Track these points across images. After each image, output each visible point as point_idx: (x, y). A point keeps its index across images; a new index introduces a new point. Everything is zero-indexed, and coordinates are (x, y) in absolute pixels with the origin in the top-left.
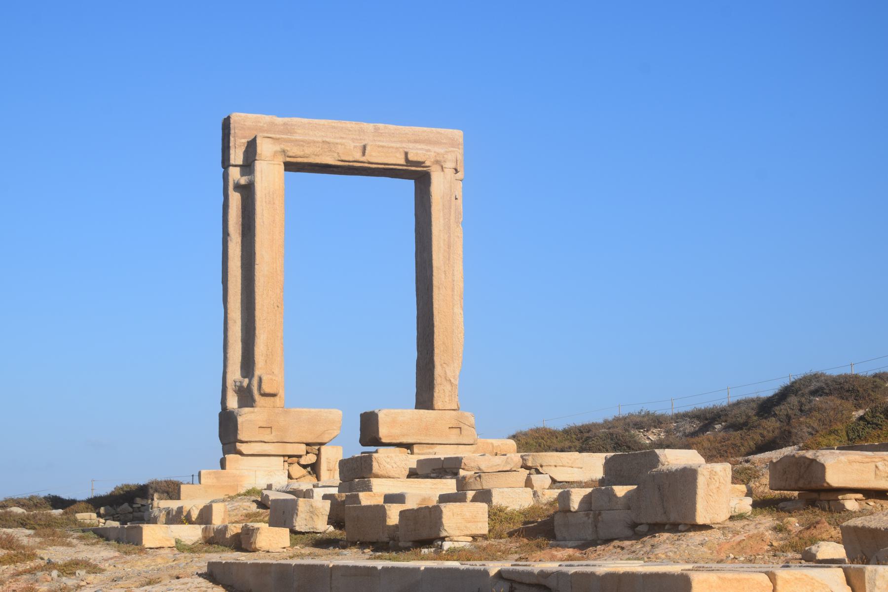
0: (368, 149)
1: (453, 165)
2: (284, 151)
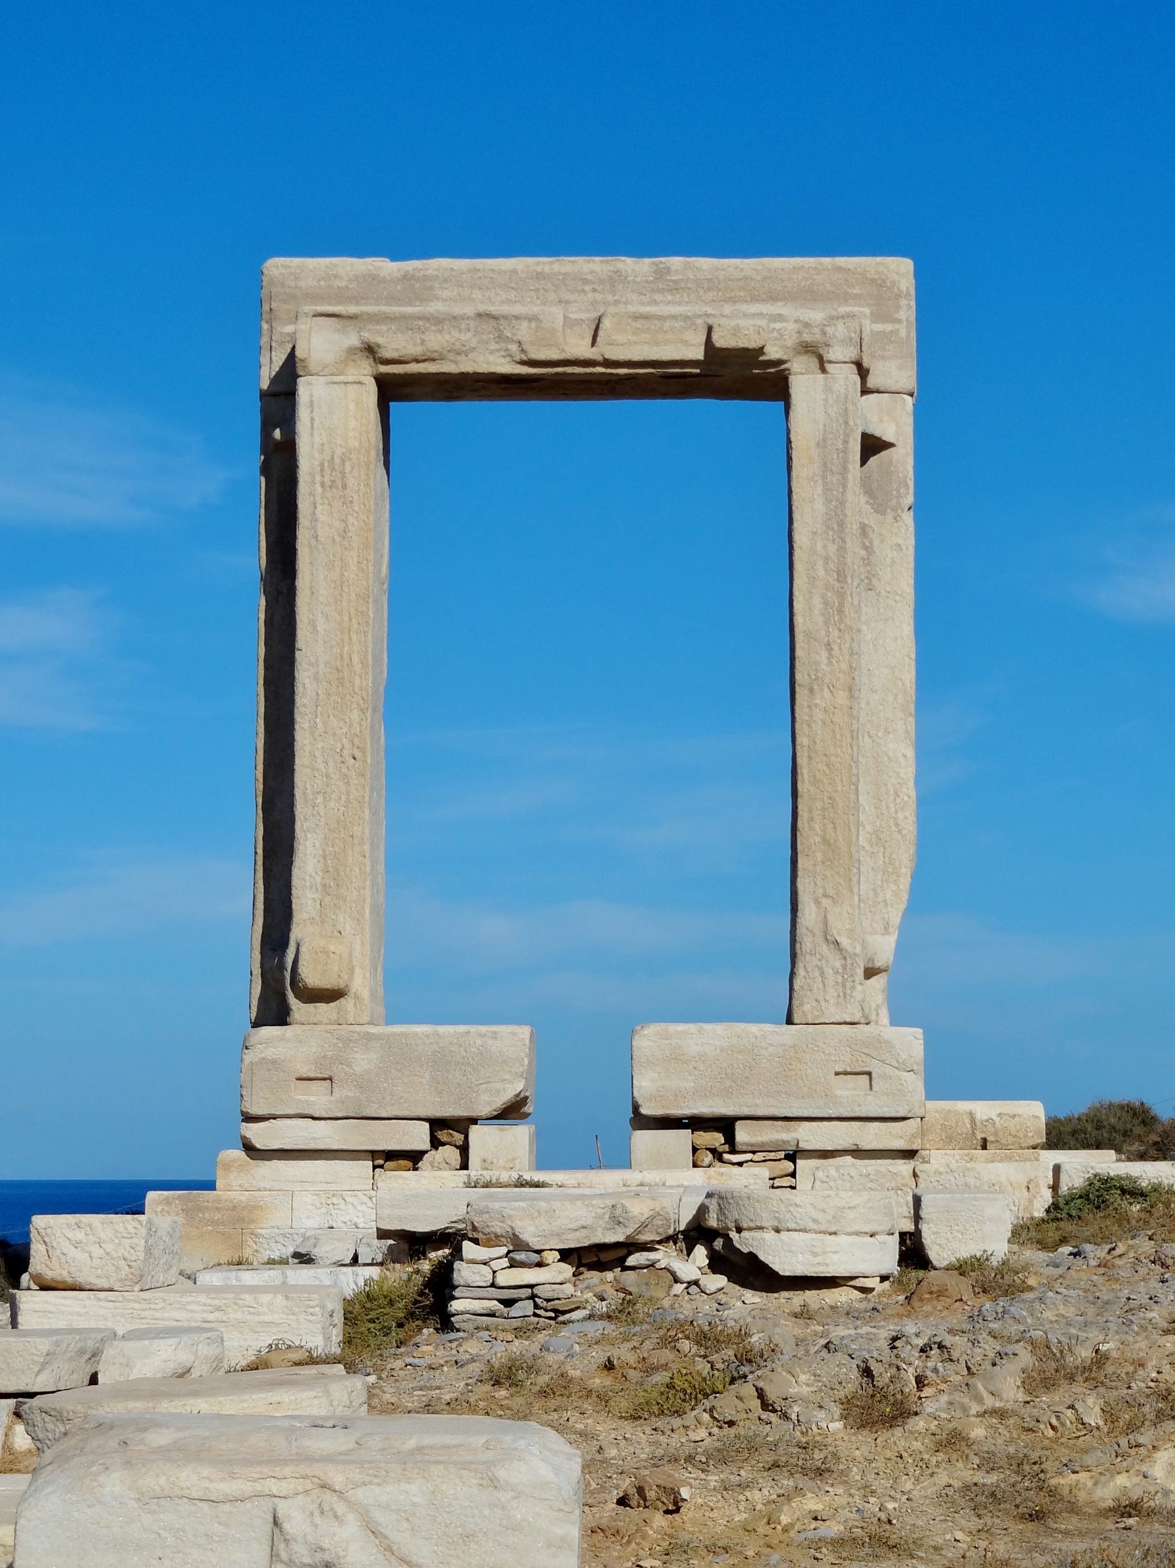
1: (851, 353)
2: (370, 350)
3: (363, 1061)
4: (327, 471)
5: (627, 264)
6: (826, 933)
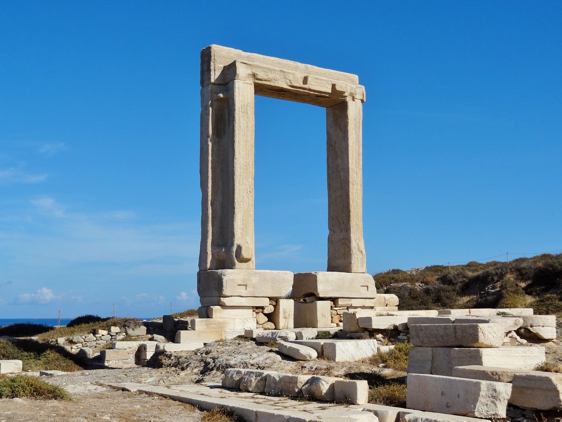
0: (309, 79)
1: (361, 97)
2: (254, 75)
3: (255, 280)
5: (299, 64)
6: (359, 249)
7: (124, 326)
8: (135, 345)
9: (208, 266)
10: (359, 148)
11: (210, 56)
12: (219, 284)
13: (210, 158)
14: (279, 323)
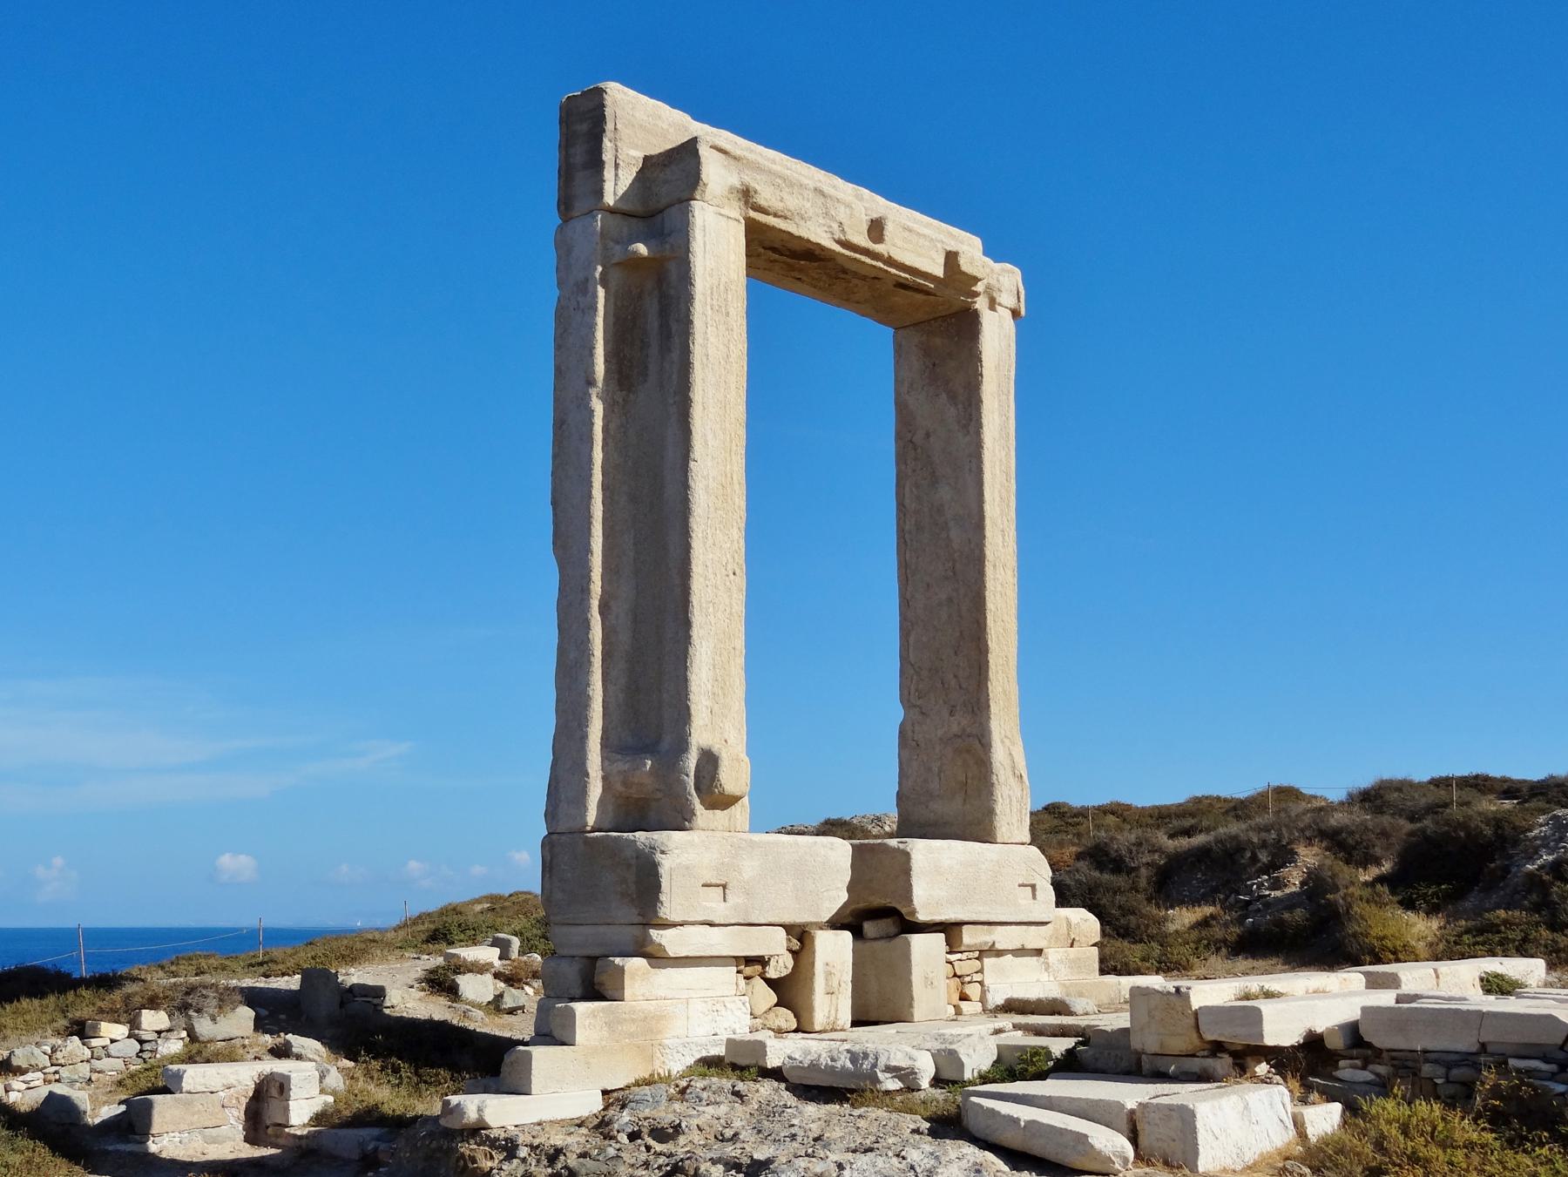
0: (889, 229)
2: (746, 194)
3: (749, 868)
4: (715, 296)
6: (1014, 768)
7: (184, 1008)
8: (244, 1076)
9: (591, 817)
10: (1008, 454)
11: (601, 119)
12: (644, 884)
13: (598, 455)
14: (811, 1009)
